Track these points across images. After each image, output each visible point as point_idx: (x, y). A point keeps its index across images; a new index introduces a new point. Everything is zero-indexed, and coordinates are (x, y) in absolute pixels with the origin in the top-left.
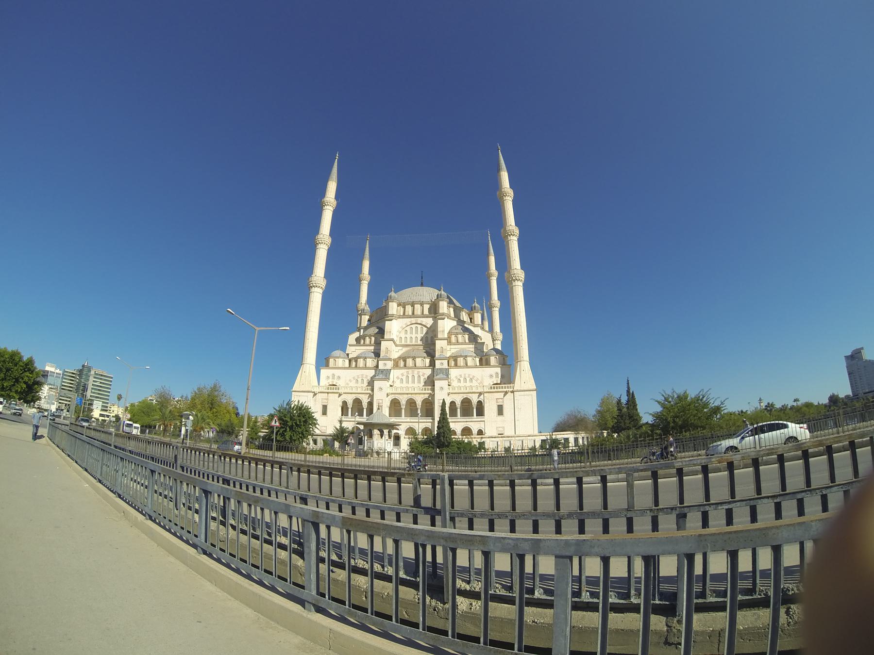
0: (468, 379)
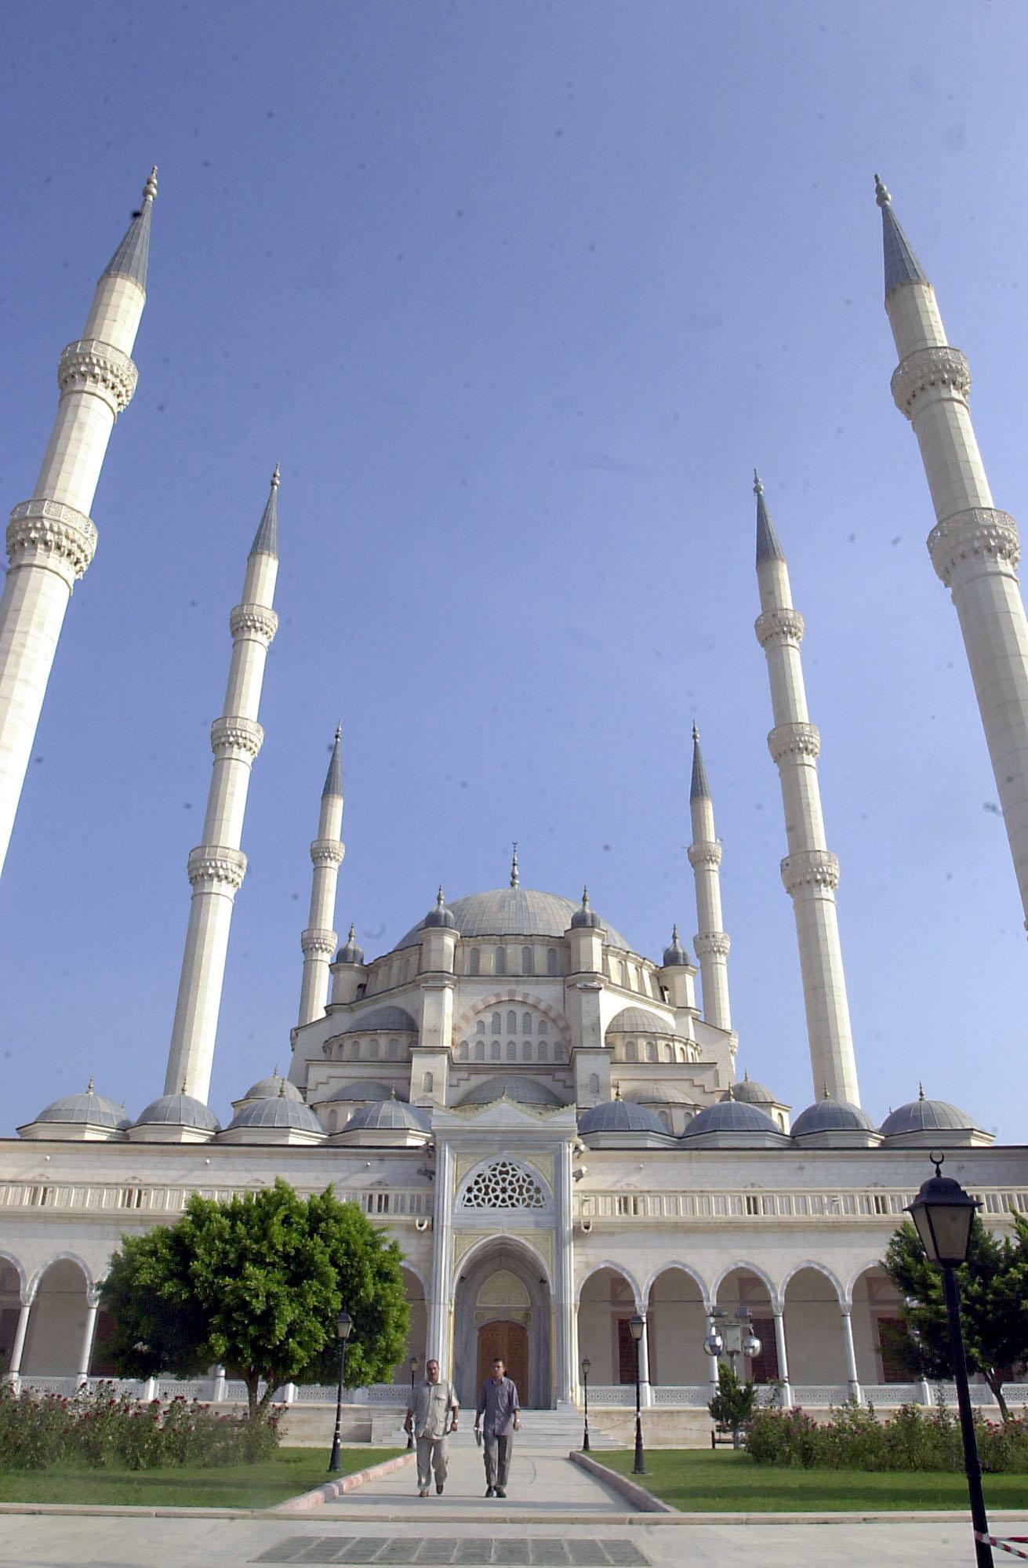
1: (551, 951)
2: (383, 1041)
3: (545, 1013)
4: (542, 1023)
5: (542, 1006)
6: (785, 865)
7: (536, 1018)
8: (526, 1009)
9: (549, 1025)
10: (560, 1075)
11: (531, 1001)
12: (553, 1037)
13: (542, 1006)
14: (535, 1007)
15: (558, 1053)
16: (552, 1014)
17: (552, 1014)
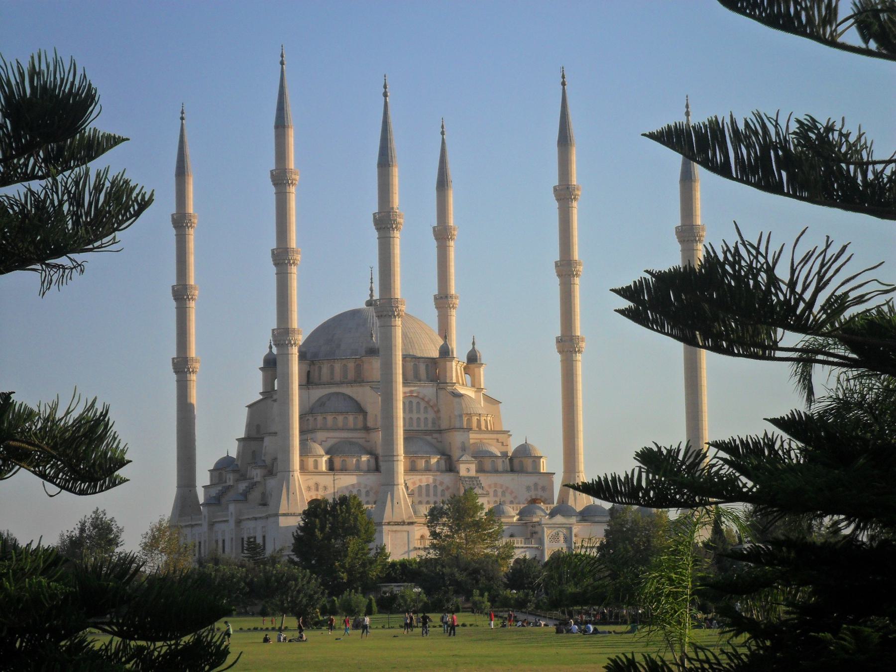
0: (500, 491)
1: (427, 366)
2: (351, 418)
3: (428, 402)
4: (425, 408)
5: (426, 399)
6: (560, 341)
7: (423, 405)
8: (418, 400)
9: (429, 409)
10: (435, 435)
11: (421, 395)
12: (431, 415)
13: (426, 399)
14: (423, 399)
15: (434, 423)
16: (431, 403)
17: (431, 403)
